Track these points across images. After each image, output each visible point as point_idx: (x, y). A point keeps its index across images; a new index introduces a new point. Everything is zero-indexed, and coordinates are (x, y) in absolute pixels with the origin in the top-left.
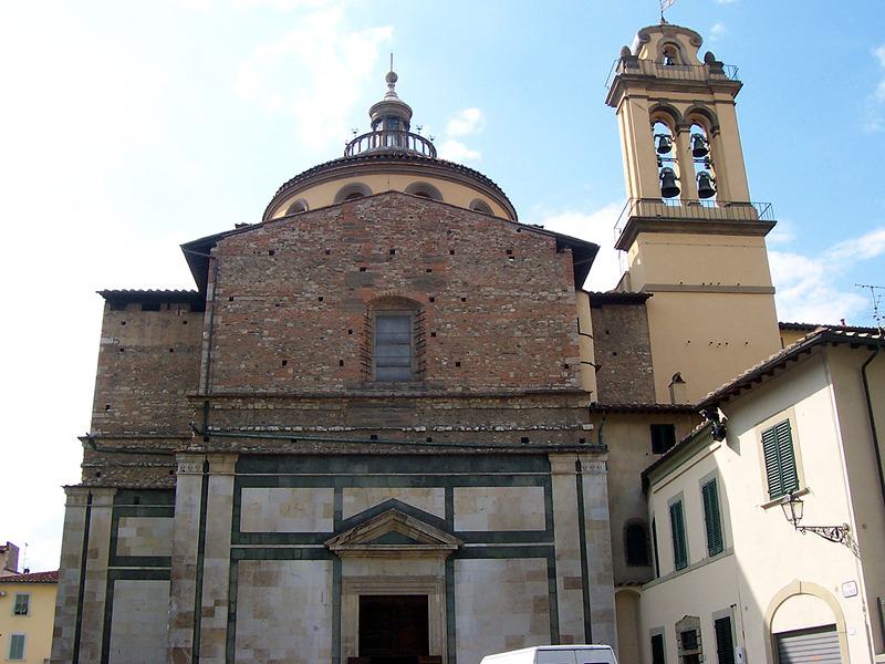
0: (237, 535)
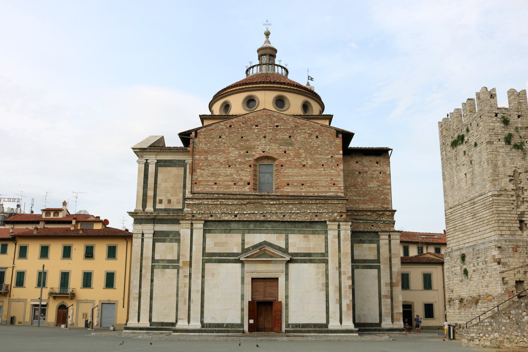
0: (204, 253)
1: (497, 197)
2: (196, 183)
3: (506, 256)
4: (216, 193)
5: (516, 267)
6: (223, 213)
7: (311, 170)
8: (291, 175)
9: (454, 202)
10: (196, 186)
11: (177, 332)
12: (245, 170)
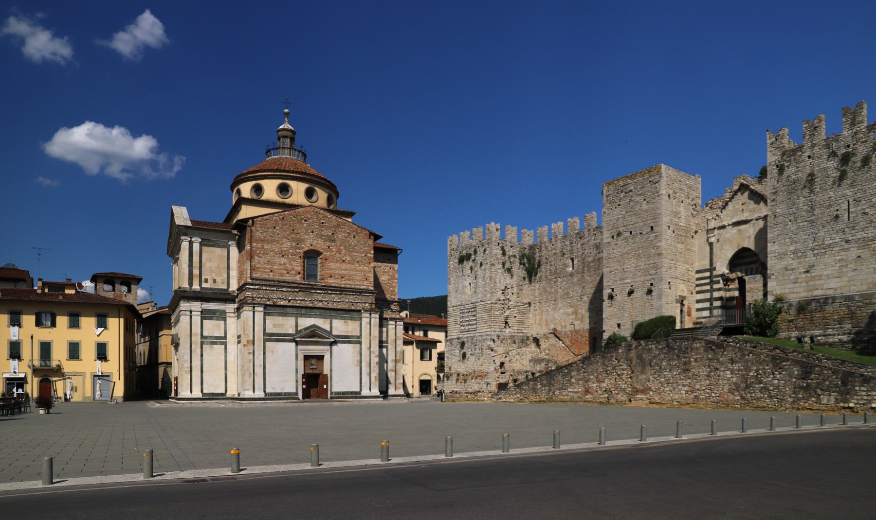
0: (265, 334)
2: (254, 269)
6: (278, 298)
8: (333, 269)
9: (457, 302)
11: (245, 401)
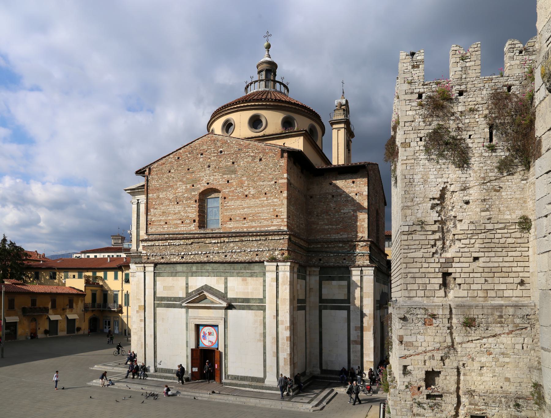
1: (406, 236)
3: (413, 332)
4: (167, 233)
5: (428, 349)
6: (171, 255)
7: (253, 200)
10: (151, 227)
12: (191, 206)
